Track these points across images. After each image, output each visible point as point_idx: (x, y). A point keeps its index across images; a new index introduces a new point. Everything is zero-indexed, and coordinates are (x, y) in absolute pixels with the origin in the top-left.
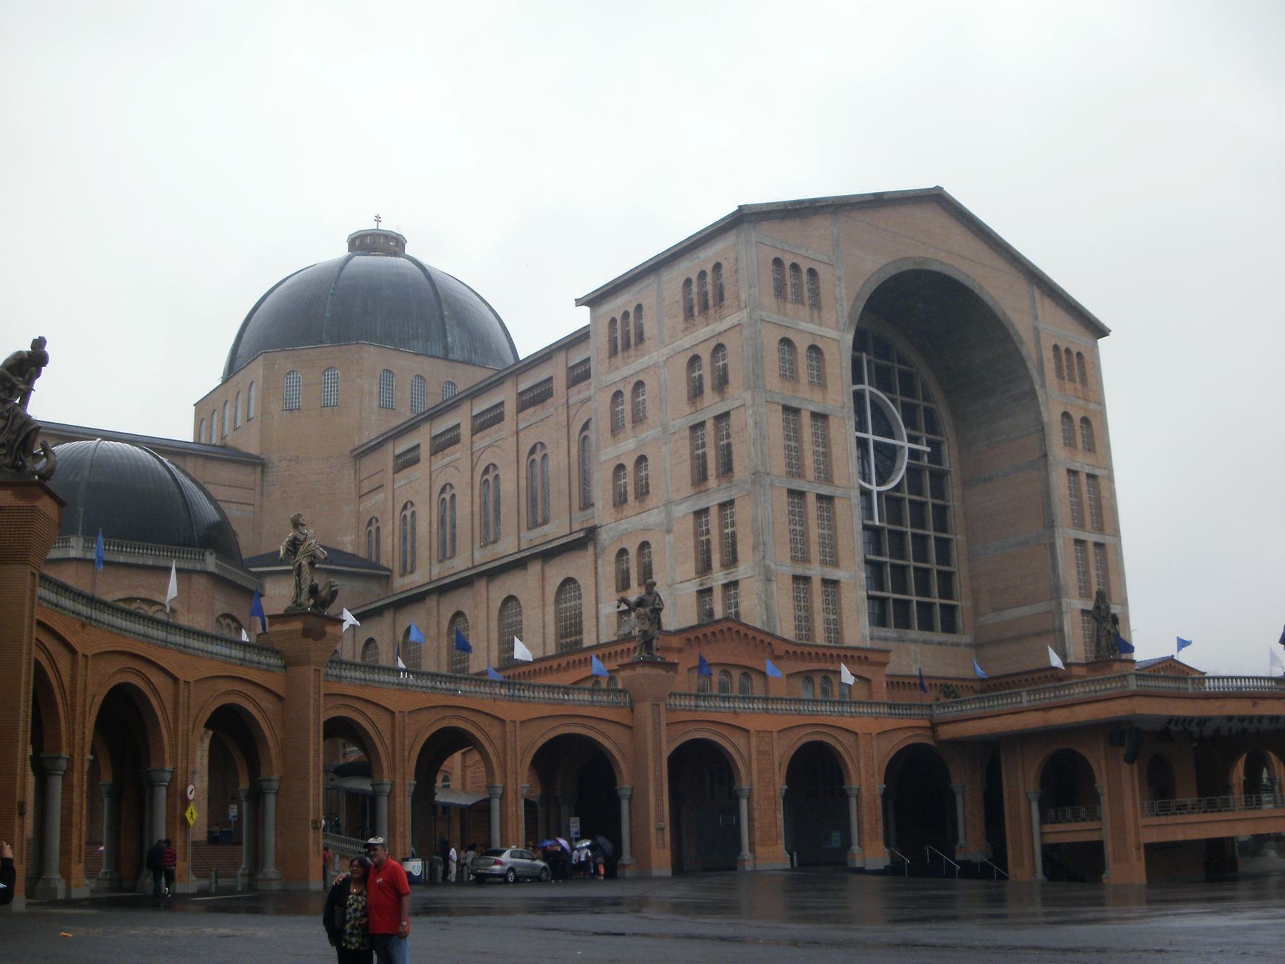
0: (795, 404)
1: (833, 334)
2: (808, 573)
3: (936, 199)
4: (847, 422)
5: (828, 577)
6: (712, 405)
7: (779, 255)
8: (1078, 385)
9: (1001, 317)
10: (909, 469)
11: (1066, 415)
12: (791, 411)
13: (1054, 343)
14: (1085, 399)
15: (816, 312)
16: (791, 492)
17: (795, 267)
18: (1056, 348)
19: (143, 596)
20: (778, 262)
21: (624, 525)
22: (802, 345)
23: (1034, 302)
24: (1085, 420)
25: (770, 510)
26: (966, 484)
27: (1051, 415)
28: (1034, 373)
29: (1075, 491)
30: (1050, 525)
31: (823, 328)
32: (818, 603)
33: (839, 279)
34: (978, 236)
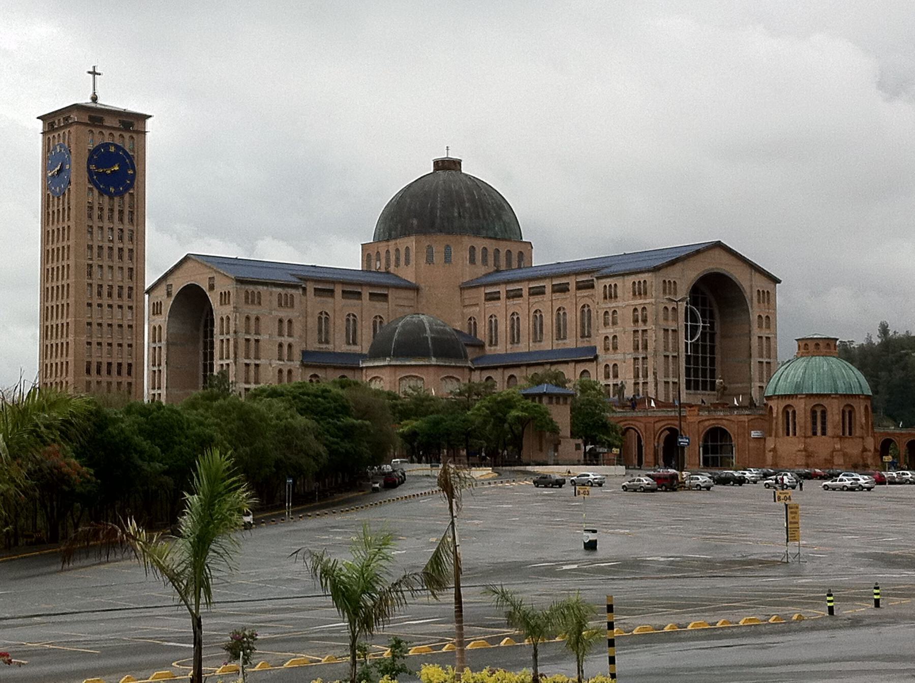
3: (719, 245)
6: (641, 327)
10: (702, 332)
11: (760, 316)
12: (666, 330)
14: (769, 309)
16: (665, 356)
18: (758, 291)
20: (664, 281)
21: (608, 356)
24: (767, 317)
26: (723, 337)
27: (754, 317)
28: (749, 305)
29: (761, 345)
30: (750, 356)
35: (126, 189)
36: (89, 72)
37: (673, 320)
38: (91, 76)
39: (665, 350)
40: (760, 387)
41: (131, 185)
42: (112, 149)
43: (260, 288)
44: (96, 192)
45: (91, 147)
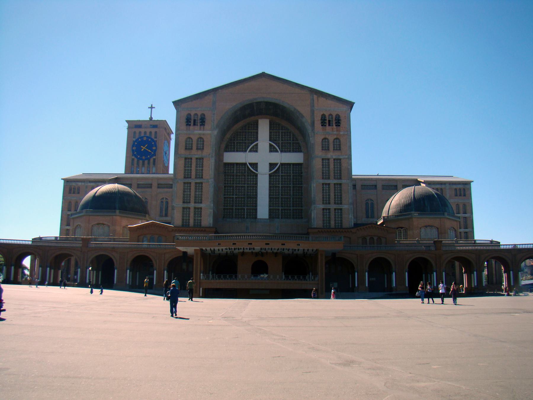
0: (189, 157)
1: (209, 132)
2: (189, 206)
3: (263, 75)
4: (211, 159)
5: (196, 207)
7: (190, 112)
8: (334, 127)
9: (293, 110)
12: (188, 161)
13: (322, 113)
15: (202, 127)
16: (184, 183)
17: (196, 114)
19: (101, 223)
20: (190, 115)
22: (195, 139)
23: (313, 101)
25: (176, 189)
28: (309, 128)
31: (205, 131)
32: (192, 214)
33: (214, 114)
34: (284, 84)
35: (150, 157)
36: (149, 108)
37: (197, 149)
38: (150, 109)
39: (185, 177)
40: (323, 209)
41: (155, 155)
42: (145, 139)
43: (80, 184)
44: (136, 160)
45: (134, 139)
